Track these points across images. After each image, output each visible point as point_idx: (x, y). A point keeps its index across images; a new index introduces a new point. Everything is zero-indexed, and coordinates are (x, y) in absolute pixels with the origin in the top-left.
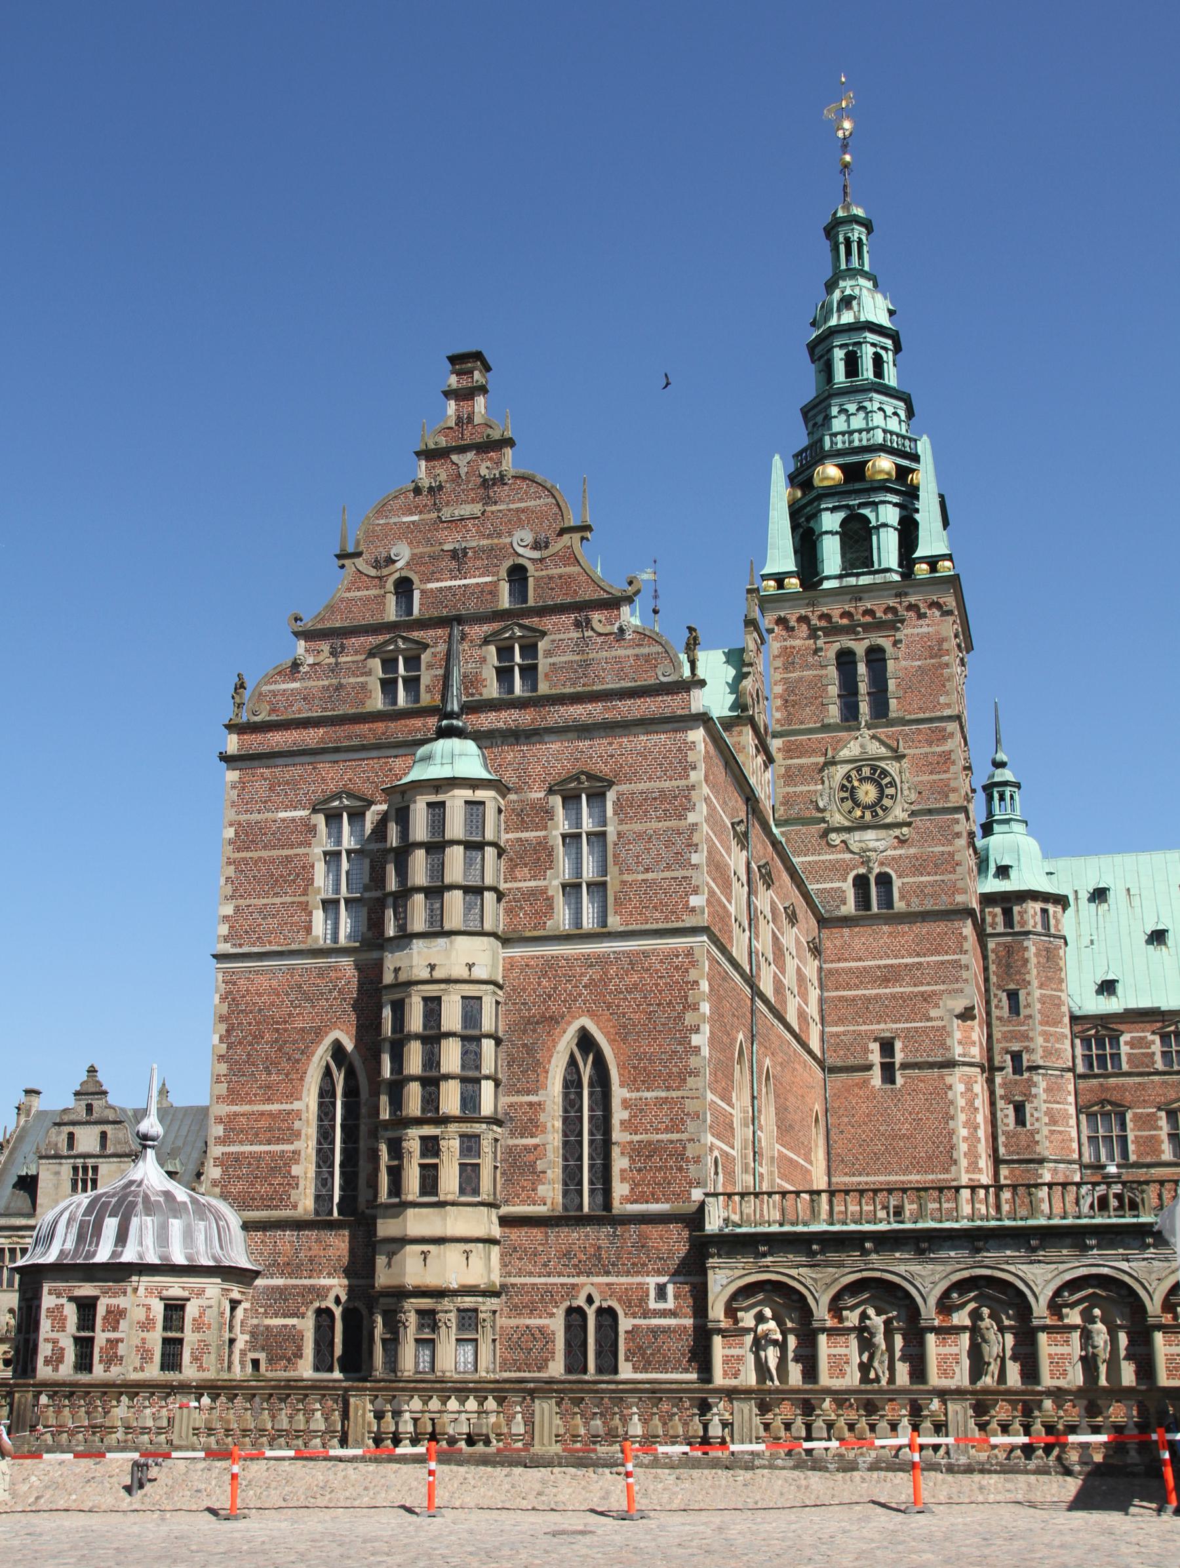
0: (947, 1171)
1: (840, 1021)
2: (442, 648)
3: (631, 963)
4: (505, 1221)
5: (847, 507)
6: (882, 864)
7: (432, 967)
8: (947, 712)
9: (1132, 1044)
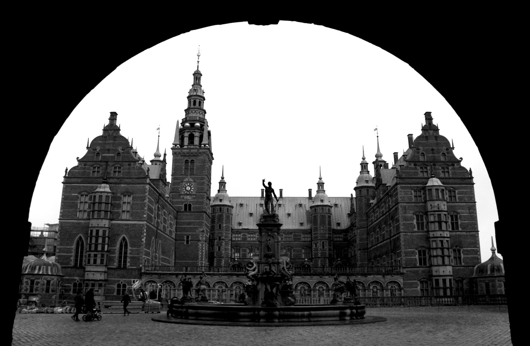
0: (197, 260)
1: (180, 231)
2: (104, 167)
3: (133, 226)
4: (108, 269)
5: (190, 132)
6: (190, 202)
7: (98, 225)
8: (205, 174)
9: (243, 235)
